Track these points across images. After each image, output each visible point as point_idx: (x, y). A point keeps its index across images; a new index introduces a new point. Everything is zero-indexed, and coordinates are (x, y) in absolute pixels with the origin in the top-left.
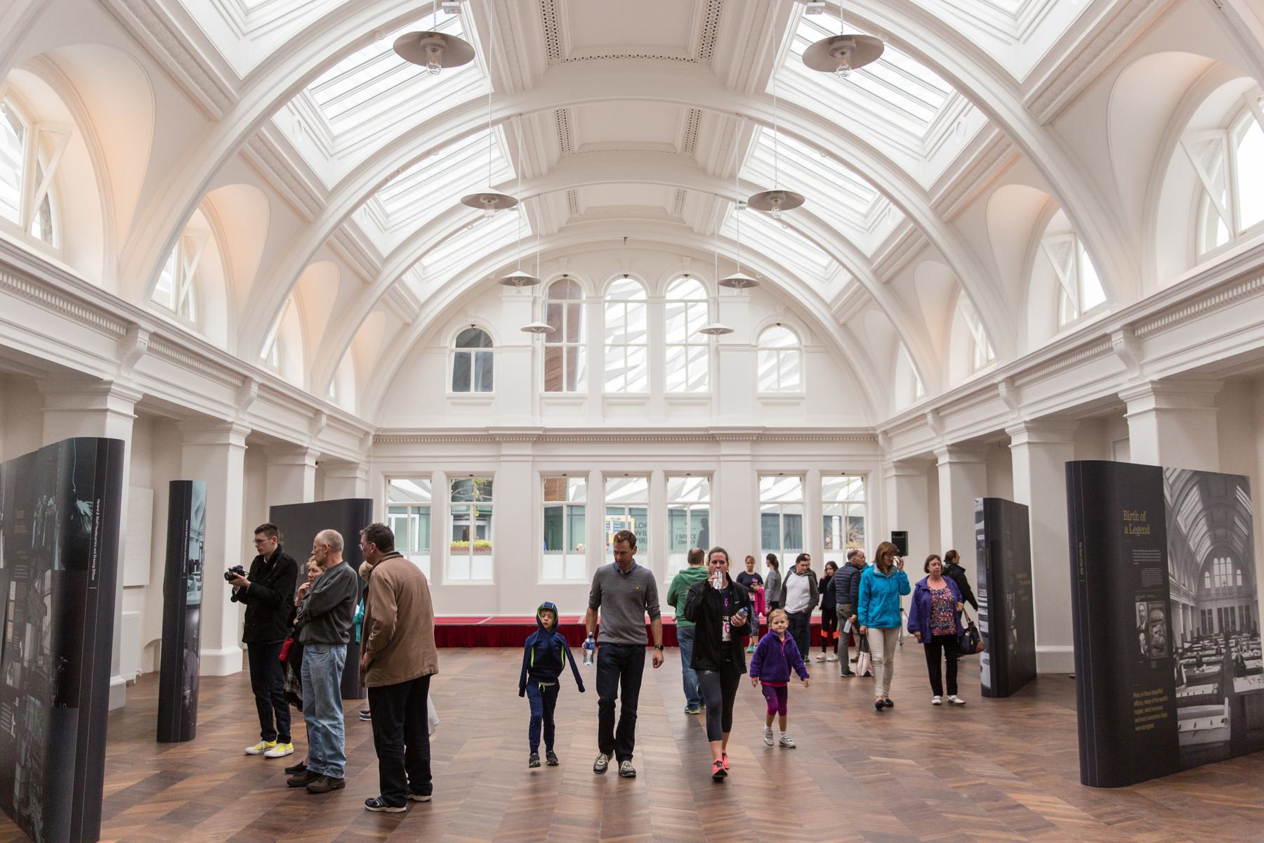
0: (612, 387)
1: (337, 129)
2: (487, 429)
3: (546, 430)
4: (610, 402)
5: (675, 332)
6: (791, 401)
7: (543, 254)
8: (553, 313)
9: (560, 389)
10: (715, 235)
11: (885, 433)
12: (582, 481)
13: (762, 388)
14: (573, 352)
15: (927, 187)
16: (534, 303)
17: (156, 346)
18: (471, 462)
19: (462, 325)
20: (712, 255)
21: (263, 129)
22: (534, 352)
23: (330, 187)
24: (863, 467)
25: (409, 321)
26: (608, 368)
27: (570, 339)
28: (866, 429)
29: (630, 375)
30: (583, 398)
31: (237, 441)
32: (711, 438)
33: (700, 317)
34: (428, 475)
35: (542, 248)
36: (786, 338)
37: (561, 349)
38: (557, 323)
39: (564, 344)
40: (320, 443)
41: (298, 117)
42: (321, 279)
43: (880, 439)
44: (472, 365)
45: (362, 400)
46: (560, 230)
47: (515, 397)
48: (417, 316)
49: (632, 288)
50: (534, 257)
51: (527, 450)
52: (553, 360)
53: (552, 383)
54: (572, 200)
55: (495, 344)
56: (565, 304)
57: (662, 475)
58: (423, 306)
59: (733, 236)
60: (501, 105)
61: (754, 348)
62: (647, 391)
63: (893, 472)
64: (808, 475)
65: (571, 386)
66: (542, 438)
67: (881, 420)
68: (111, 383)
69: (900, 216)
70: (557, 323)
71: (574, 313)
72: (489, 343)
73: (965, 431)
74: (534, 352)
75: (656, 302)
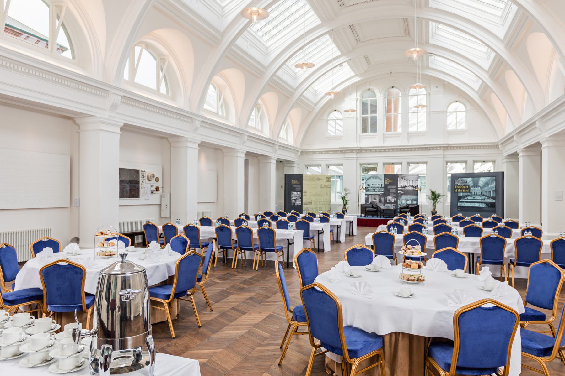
0: (412, 129)
1: (268, 44)
2: (340, 148)
3: (361, 148)
10: (428, 67)
11: (502, 144)
12: (399, 166)
13: (450, 128)
16: (357, 100)
17: (204, 125)
21: (232, 47)
22: (357, 119)
23: (266, 66)
24: (493, 159)
26: (410, 123)
28: (494, 143)
30: (399, 134)
32: (426, 148)
34: (320, 165)
36: (460, 106)
37: (367, 117)
40: (275, 155)
41: (250, 42)
43: (500, 146)
45: (295, 141)
46: (365, 72)
48: (314, 109)
51: (354, 155)
52: (364, 121)
58: (316, 105)
60: (325, 28)
63: (505, 160)
64: (496, 162)
66: (360, 151)
73: (528, 142)
74: (357, 119)
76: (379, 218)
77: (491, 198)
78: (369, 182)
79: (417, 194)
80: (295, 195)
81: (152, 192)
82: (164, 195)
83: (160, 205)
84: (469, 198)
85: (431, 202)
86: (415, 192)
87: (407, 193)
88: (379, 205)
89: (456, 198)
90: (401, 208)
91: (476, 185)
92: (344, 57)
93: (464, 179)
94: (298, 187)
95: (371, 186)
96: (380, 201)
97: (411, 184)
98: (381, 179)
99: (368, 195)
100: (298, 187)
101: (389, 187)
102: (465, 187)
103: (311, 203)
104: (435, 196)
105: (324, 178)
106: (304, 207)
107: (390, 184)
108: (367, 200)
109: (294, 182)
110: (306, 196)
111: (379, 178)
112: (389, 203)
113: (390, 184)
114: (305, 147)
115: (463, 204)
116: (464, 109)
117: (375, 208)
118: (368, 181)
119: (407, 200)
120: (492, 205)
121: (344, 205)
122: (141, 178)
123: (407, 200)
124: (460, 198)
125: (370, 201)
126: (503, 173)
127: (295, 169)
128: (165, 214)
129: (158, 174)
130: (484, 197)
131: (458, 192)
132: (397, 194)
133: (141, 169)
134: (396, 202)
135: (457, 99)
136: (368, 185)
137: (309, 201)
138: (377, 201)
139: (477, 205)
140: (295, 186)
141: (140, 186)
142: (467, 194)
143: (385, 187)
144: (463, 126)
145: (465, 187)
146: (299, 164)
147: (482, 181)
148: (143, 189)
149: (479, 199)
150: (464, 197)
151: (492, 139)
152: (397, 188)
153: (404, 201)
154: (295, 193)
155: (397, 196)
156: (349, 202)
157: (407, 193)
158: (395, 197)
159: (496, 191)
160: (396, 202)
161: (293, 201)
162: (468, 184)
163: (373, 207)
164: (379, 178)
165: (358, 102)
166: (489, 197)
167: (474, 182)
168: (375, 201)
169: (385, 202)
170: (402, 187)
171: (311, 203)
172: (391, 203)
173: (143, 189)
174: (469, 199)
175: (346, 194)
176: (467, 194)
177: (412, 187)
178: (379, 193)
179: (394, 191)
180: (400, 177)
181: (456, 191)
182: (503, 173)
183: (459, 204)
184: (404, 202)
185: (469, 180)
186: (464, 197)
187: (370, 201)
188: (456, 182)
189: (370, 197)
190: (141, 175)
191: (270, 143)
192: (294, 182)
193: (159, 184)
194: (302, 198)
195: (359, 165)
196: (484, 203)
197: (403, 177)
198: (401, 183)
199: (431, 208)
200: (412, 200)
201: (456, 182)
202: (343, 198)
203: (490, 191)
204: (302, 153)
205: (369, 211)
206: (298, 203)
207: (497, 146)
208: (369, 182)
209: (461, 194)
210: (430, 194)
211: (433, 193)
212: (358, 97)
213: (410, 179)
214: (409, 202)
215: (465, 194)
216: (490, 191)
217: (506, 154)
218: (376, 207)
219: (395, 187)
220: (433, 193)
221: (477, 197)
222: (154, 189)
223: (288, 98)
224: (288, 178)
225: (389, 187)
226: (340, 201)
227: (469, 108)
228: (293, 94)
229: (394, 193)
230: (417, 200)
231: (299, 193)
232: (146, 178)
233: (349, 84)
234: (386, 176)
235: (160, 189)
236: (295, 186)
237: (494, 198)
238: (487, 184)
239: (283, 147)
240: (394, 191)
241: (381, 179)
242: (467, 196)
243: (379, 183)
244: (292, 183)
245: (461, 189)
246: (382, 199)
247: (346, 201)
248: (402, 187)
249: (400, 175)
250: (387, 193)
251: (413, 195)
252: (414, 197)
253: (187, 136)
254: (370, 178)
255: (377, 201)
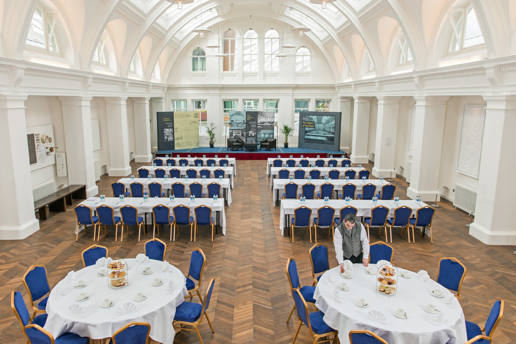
2: (204, 85)
3: (224, 85)
4: (244, 75)
5: (267, 49)
6: (307, 74)
7: (221, 22)
8: (226, 43)
9: (228, 70)
11: (338, 87)
14: (233, 57)
15: (357, 11)
16: (219, 40)
17: (95, 80)
18: (199, 95)
19: (195, 47)
20: (281, 21)
21: (123, 2)
23: (146, 13)
25: (176, 48)
27: (231, 53)
29: (253, 48)
31: (124, 102)
33: (276, 45)
35: (221, 20)
37: (228, 56)
38: (227, 46)
39: (230, 54)
42: (146, 43)
44: (199, 56)
45: (162, 77)
46: (228, 13)
47: (212, 71)
48: (179, 46)
49: (253, 34)
50: (218, 23)
51: (217, 92)
53: (225, 68)
54: (232, 5)
55: (207, 54)
56: (230, 39)
57: (262, 101)
59: (288, 15)
61: (295, 56)
62: (257, 71)
63: (340, 100)
65: (232, 69)
66: (223, 88)
67: (337, 83)
68: (82, 97)
69: (346, 19)
70: (227, 46)
71: (233, 42)
72: (204, 54)
75: (261, 38)
76: (244, 152)
77: (331, 133)
78: (233, 118)
79: (273, 129)
80: (167, 131)
81: (48, 153)
82: (58, 155)
83: (55, 165)
84: (314, 132)
85: (284, 135)
86: (271, 126)
87: (265, 128)
88: (242, 138)
89: (303, 131)
90: (261, 142)
91: (320, 122)
92: (214, 3)
93: (311, 116)
94: (170, 124)
95: (235, 121)
96: (243, 135)
97: (269, 120)
98: (243, 116)
99: (232, 130)
100: (170, 124)
101: (250, 123)
102: (311, 123)
103: (182, 138)
104: (287, 130)
105: (193, 115)
106: (176, 142)
107: (252, 120)
108: (231, 134)
109: (166, 119)
110: (177, 132)
111: (242, 115)
112: (250, 137)
113: (252, 120)
114: (172, 83)
115: (309, 137)
116: (309, 54)
117: (240, 143)
118: (232, 118)
119: (265, 134)
120: (332, 139)
121: (212, 139)
122: (36, 142)
123: (265, 134)
124: (306, 132)
125: (234, 135)
126: (341, 113)
127: (164, 105)
128: (62, 173)
129: (51, 135)
130: (325, 132)
131: (305, 127)
132: (257, 129)
133: (35, 133)
134: (256, 136)
135: (304, 45)
136: (232, 121)
137: (180, 136)
138: (240, 135)
139: (320, 138)
140: (167, 123)
141: (37, 150)
142: (312, 129)
143: (247, 123)
144: (308, 70)
145: (311, 123)
146: (166, 99)
147: (325, 119)
148: (39, 152)
149: (321, 133)
150: (310, 131)
151: (329, 82)
152: (257, 123)
153: (263, 135)
154: (167, 130)
155: (257, 130)
156: (215, 136)
157: (265, 128)
158: (255, 131)
159: (335, 128)
160: (256, 136)
161: (166, 137)
162: (313, 121)
163: (237, 142)
164: (242, 115)
165: (221, 41)
166: (329, 132)
167: (318, 119)
168: (238, 135)
169: (247, 136)
170: (261, 123)
171: (182, 138)
172: (252, 136)
173: (39, 152)
174: (314, 133)
175: (213, 129)
176: (312, 129)
177: (269, 122)
178: (242, 128)
179: (254, 126)
180: (260, 114)
181: (304, 126)
182: (341, 113)
183: (306, 137)
184: (262, 135)
185: (314, 118)
186: (310, 131)
187: (234, 135)
188: (304, 119)
189: (234, 131)
190: (35, 139)
191: (145, 85)
192: (166, 119)
193: (52, 145)
194: (173, 134)
195: (221, 101)
196: (326, 137)
197: (262, 114)
198: (261, 120)
199: (284, 141)
200: (270, 134)
201: (304, 119)
202: (210, 132)
203: (330, 128)
204: (168, 88)
205: (235, 146)
206: (170, 139)
207: (334, 88)
208: (233, 118)
209: (307, 129)
210: (283, 128)
211: (286, 128)
212: (220, 36)
213: (267, 116)
214: (267, 136)
215: (311, 129)
216: (330, 128)
217: (340, 95)
218: (241, 141)
219: (255, 123)
220: (286, 128)
221: (320, 132)
222: (48, 150)
223: (160, 39)
224: (160, 115)
225: (250, 123)
226: (208, 135)
227: (313, 53)
228: (165, 36)
229: (254, 128)
230: (273, 134)
231: (171, 129)
232: (40, 141)
233: (212, 24)
234: (248, 113)
235: (54, 149)
236: (167, 123)
237: (333, 133)
238: (328, 122)
239: (156, 86)
240: (254, 126)
241: (243, 116)
242: (312, 131)
243: (242, 119)
244: (164, 120)
245: (308, 125)
246: (245, 133)
247: (213, 135)
248: (261, 123)
249: (260, 112)
250: (248, 128)
251: (270, 129)
252: (271, 131)
253: (80, 96)
254: (234, 115)
255: (240, 135)
